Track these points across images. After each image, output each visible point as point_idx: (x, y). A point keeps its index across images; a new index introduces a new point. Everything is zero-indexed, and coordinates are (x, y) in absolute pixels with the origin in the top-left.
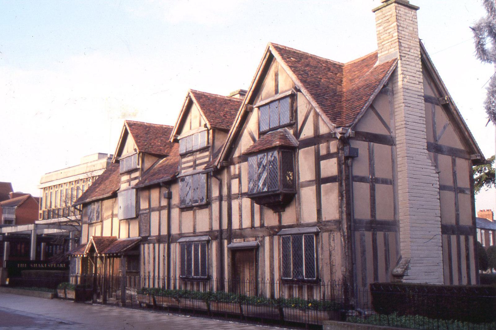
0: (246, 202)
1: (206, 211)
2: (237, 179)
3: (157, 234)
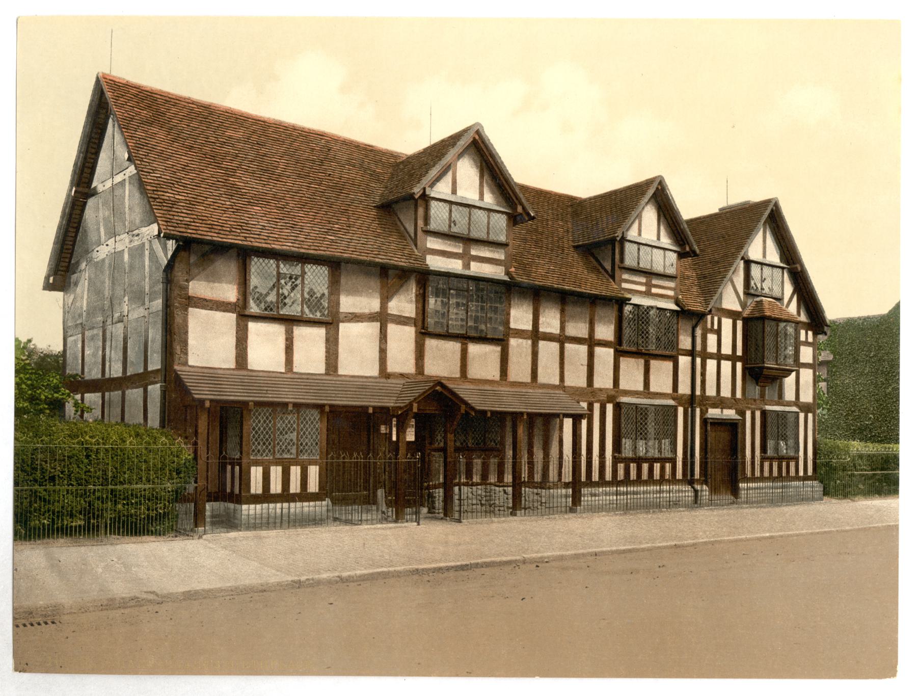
0: (726, 366)
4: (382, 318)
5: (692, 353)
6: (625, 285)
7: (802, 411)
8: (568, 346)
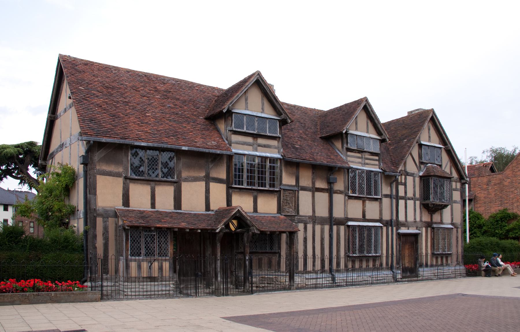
1: (376, 204)
2: (403, 186)
3: (310, 214)
4: (208, 179)
5: (389, 196)
6: (349, 159)
7: (384, 226)
8: (317, 194)
